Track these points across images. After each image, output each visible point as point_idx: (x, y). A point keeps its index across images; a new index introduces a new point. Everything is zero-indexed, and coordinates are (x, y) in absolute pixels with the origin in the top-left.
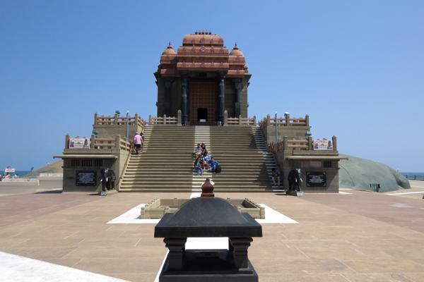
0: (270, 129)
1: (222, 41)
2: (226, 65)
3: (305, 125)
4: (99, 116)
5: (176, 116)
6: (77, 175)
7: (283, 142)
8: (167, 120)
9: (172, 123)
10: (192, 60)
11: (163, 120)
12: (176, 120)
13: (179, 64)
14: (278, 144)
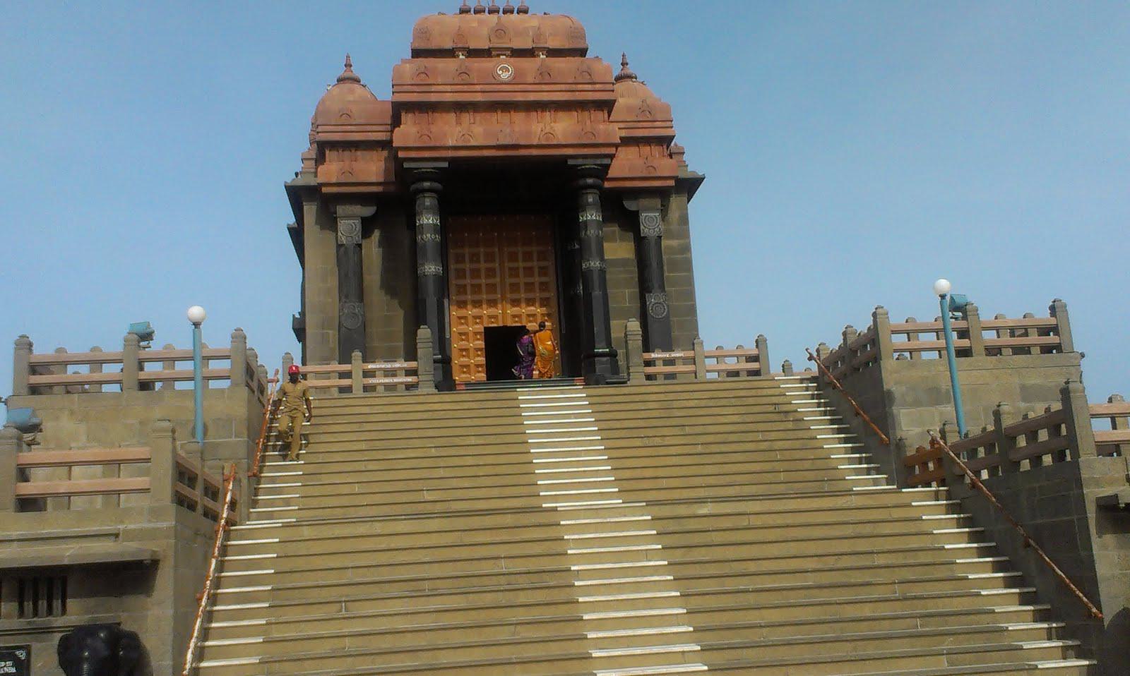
0: (893, 374)
1: (583, 37)
3: (1058, 348)
4: (43, 350)
5: (411, 355)
8: (367, 374)
10: (460, 107)
11: (347, 375)
12: (409, 372)
13: (409, 133)
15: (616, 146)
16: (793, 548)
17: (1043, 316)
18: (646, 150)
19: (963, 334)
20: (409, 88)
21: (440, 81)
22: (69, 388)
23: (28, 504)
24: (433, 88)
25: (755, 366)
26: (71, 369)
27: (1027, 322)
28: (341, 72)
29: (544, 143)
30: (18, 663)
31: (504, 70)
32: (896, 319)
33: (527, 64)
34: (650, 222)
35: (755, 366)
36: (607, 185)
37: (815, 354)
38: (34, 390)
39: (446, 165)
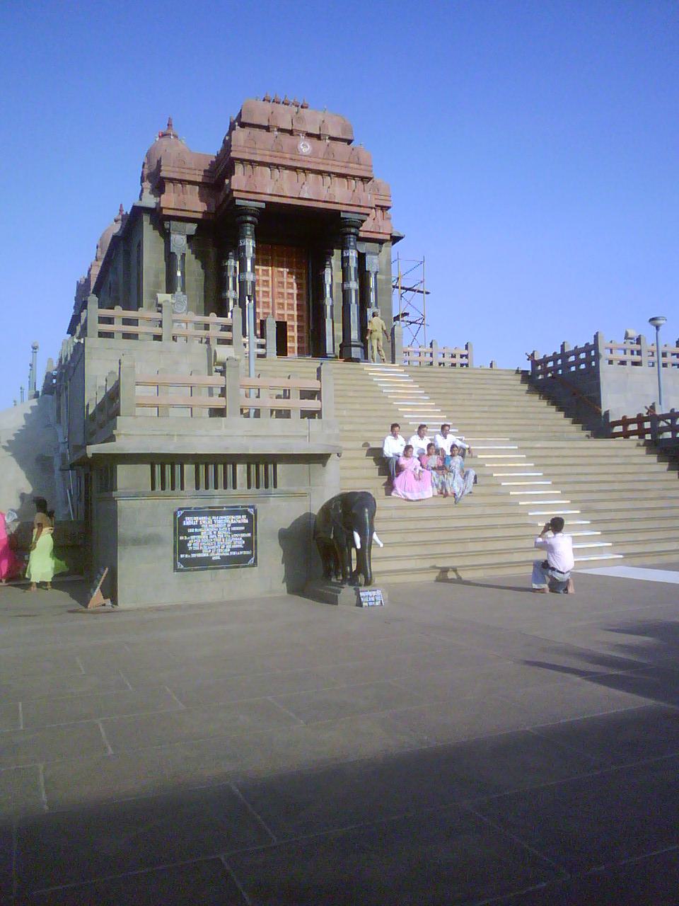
2: (367, 196)
6: (180, 529)
28: (164, 129)
30: (249, 516)
31: (305, 147)
39: (263, 205)
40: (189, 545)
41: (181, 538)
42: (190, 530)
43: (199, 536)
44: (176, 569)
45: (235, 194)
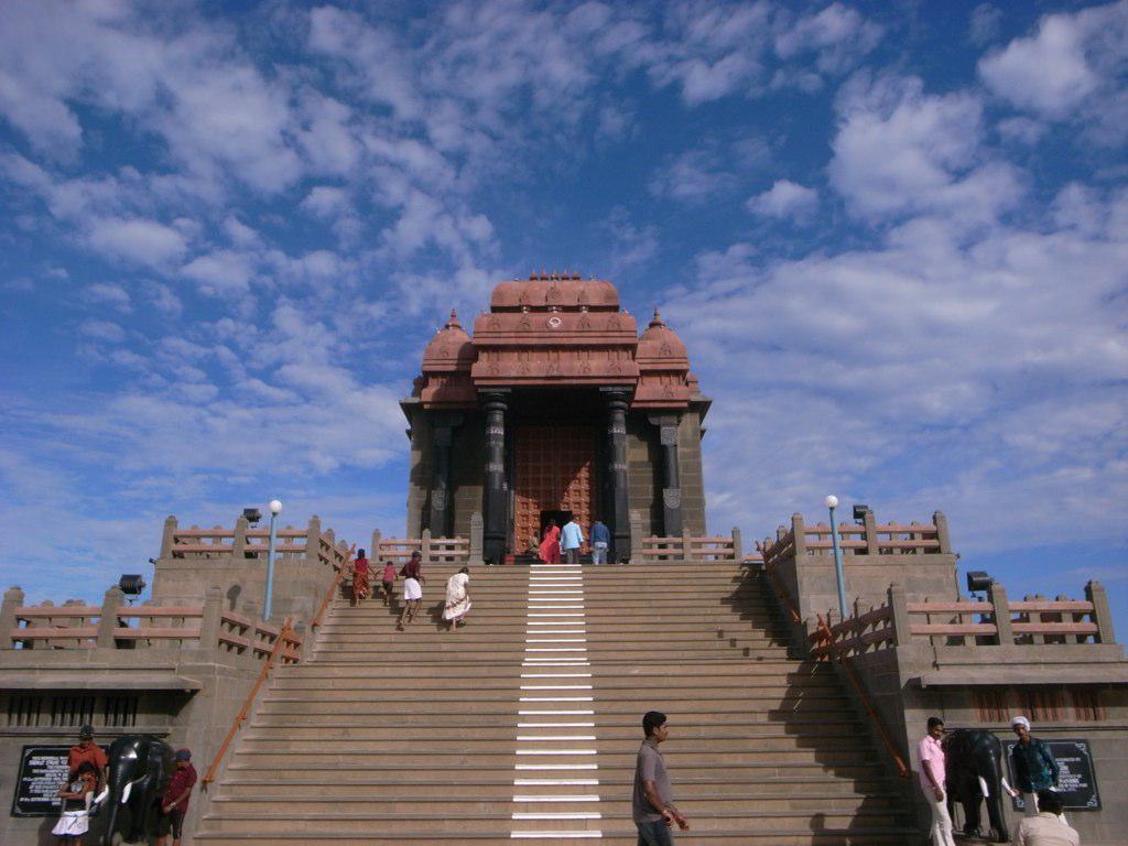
2: (628, 365)
3: (936, 550)
4: (184, 527)
6: (27, 770)
7: (887, 614)
8: (435, 547)
9: (449, 559)
12: (464, 547)
14: (858, 623)
15: (637, 378)
16: (695, 706)
17: (929, 526)
18: (666, 380)
19: (864, 536)
20: (485, 335)
21: (507, 329)
22: (207, 554)
23: (124, 643)
24: (503, 335)
25: (730, 551)
26: (203, 540)
27: (912, 528)
29: (582, 375)
31: (555, 321)
32: (810, 522)
33: (574, 317)
34: (670, 434)
35: (730, 551)
36: (634, 405)
37: (762, 546)
38: (178, 555)
39: (510, 390)
40: (31, 787)
41: (25, 779)
42: (35, 771)
43: (44, 779)
44: (14, 814)
45: (476, 383)
